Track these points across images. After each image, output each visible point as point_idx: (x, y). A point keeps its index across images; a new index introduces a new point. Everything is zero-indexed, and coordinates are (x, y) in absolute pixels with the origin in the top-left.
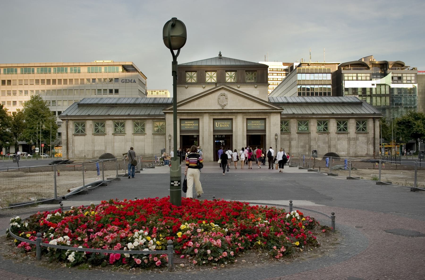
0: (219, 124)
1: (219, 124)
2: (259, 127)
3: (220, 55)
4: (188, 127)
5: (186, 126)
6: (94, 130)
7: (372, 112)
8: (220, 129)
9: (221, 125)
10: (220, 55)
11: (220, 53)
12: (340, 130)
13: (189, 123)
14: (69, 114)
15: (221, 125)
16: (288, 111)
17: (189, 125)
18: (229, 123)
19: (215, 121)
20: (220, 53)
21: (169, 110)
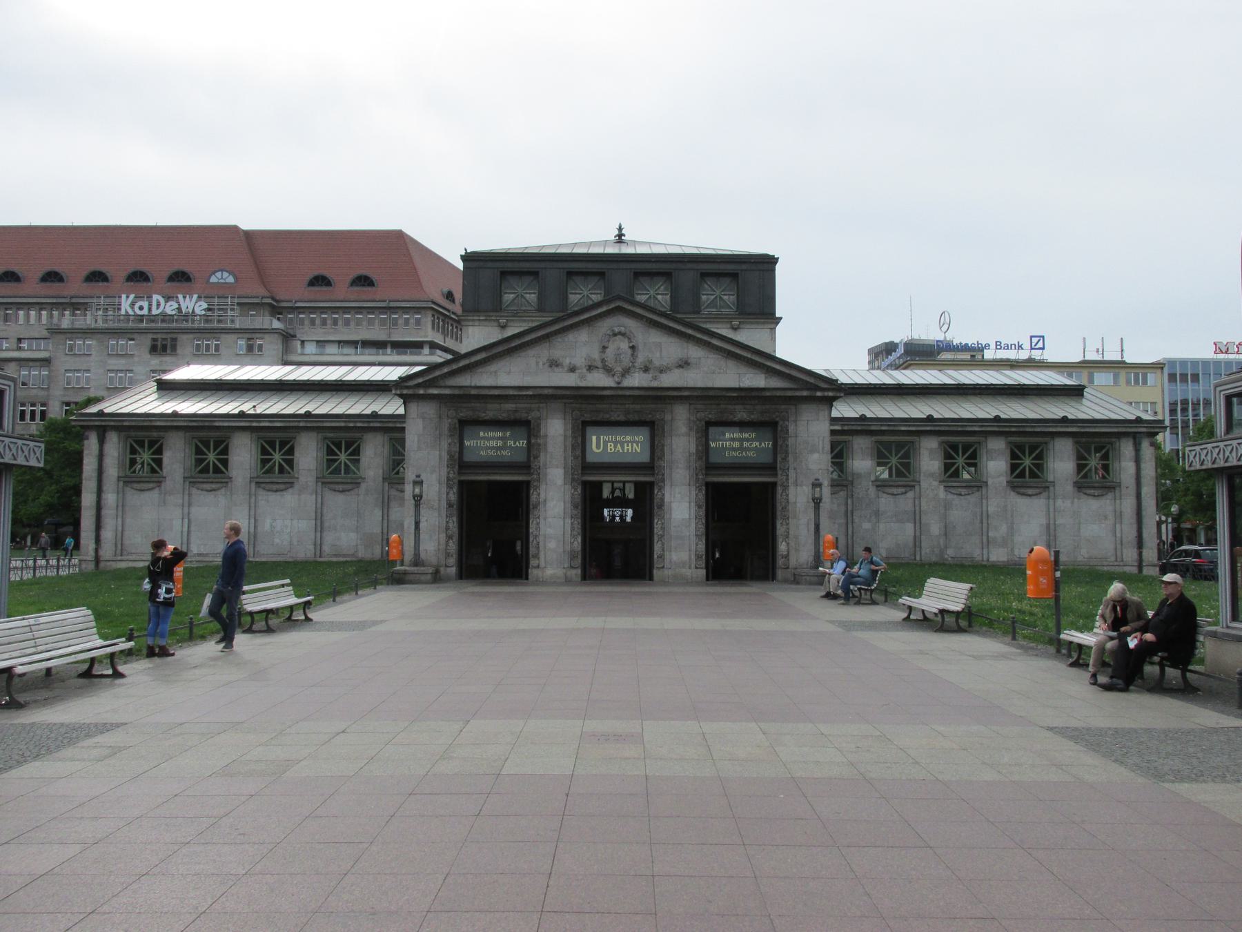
0: (605, 443)
1: (605, 443)
2: (751, 454)
3: (620, 235)
4: (491, 453)
5: (482, 449)
6: (191, 462)
7: (1133, 418)
8: (606, 459)
9: (610, 447)
10: (620, 235)
11: (620, 229)
12: (1021, 475)
13: (493, 439)
14: (106, 411)
15: (610, 447)
16: (845, 409)
17: (492, 443)
18: (640, 438)
19: (589, 430)
20: (620, 229)
21: (418, 386)
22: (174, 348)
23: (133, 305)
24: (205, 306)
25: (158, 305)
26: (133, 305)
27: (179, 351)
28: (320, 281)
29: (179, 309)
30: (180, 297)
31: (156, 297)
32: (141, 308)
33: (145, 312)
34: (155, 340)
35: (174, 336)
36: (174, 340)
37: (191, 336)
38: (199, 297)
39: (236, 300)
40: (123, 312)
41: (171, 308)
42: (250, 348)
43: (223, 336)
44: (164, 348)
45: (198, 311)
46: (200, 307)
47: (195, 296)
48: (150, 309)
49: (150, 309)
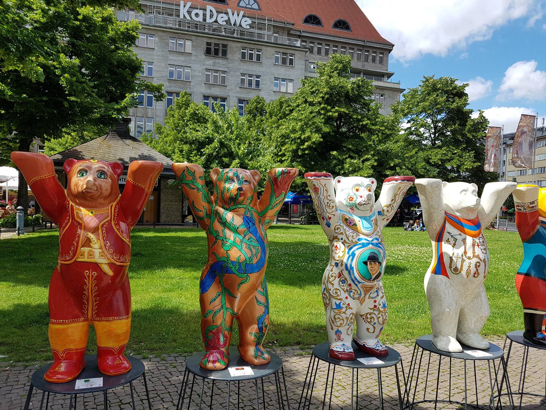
22: (225, 53)
23: (189, 13)
24: (249, 21)
25: (211, 16)
26: (189, 13)
27: (229, 56)
28: (312, 20)
29: (228, 22)
30: (229, 11)
31: (209, 8)
32: (197, 15)
33: (200, 19)
34: (208, 44)
35: (225, 43)
36: (225, 46)
37: (240, 45)
38: (244, 16)
39: (272, 23)
40: (182, 17)
41: (222, 19)
42: (284, 61)
43: (264, 48)
44: (216, 52)
45: (244, 25)
46: (246, 23)
47: (242, 13)
48: (205, 20)
49: (205, 20)
